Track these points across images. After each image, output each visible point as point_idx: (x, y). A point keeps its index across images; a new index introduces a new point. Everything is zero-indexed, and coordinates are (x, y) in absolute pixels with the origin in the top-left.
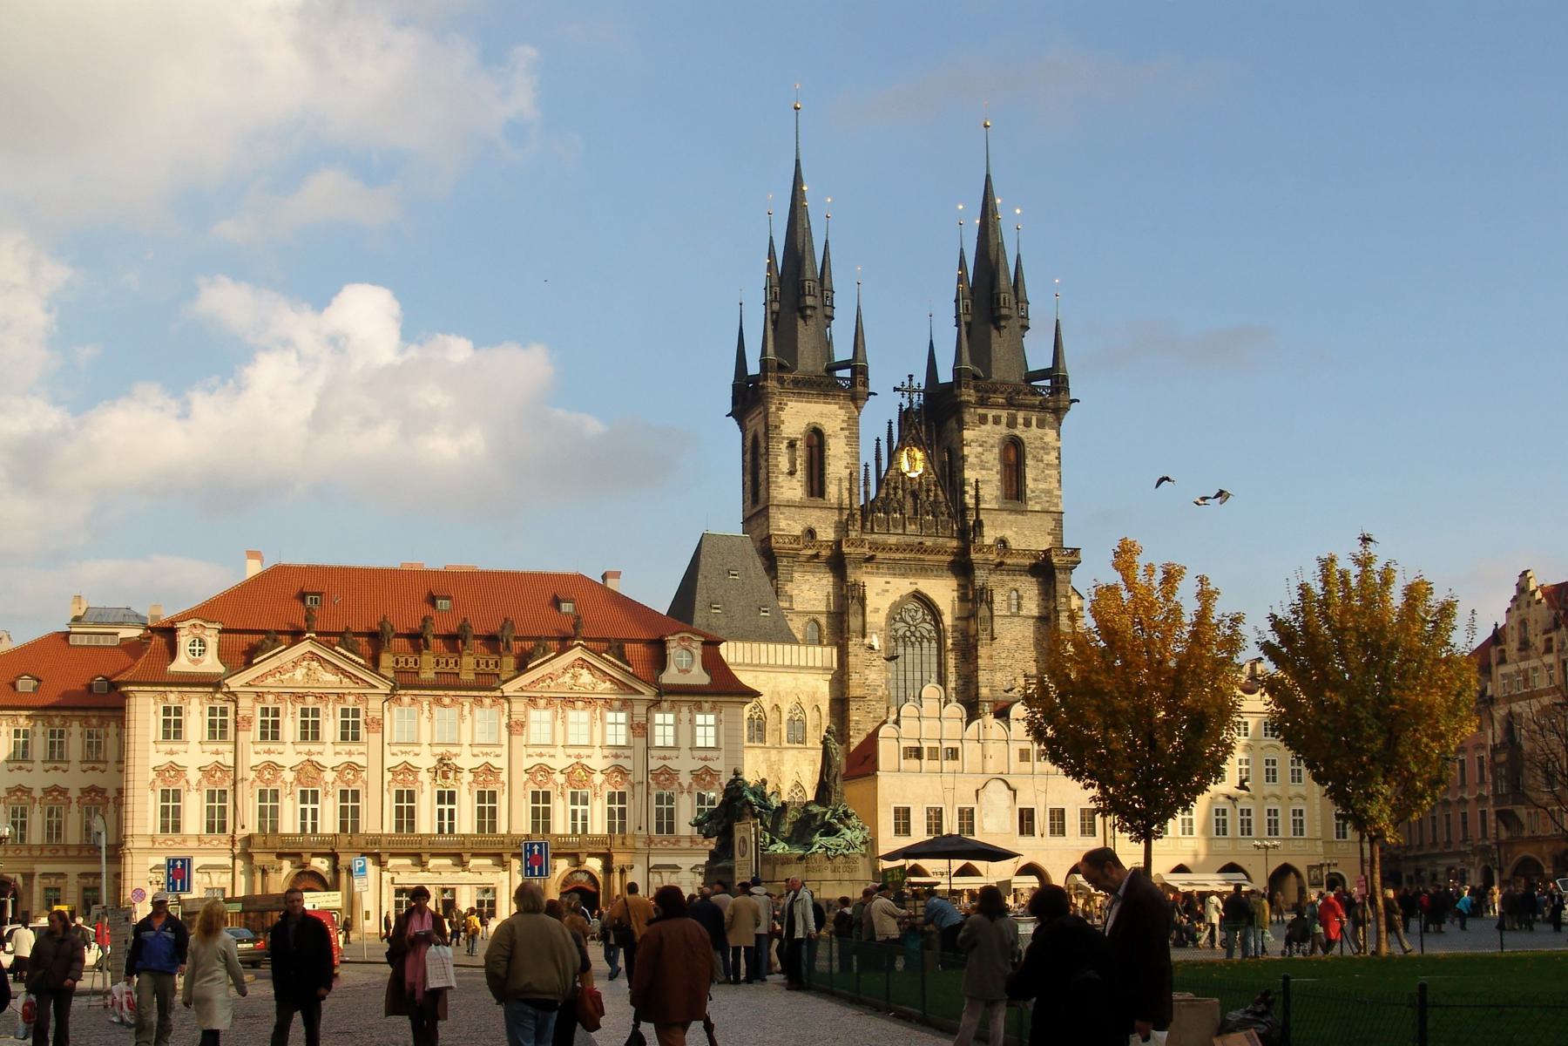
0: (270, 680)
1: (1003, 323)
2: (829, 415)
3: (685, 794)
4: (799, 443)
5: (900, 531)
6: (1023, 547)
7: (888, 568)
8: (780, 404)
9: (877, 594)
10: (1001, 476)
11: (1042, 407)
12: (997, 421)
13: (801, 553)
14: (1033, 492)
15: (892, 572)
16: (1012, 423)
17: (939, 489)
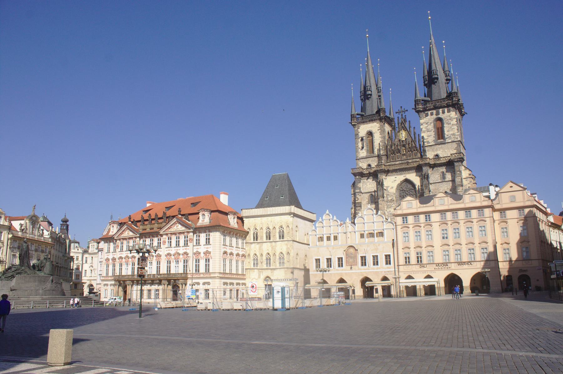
0: (122, 236)
1: (436, 80)
2: (374, 127)
3: (202, 259)
4: (364, 138)
5: (399, 159)
6: (446, 156)
7: (396, 173)
8: (358, 127)
9: (392, 182)
10: (435, 133)
11: (448, 106)
12: (432, 114)
13: (365, 173)
14: (447, 135)
15: (397, 173)
17: (413, 142)
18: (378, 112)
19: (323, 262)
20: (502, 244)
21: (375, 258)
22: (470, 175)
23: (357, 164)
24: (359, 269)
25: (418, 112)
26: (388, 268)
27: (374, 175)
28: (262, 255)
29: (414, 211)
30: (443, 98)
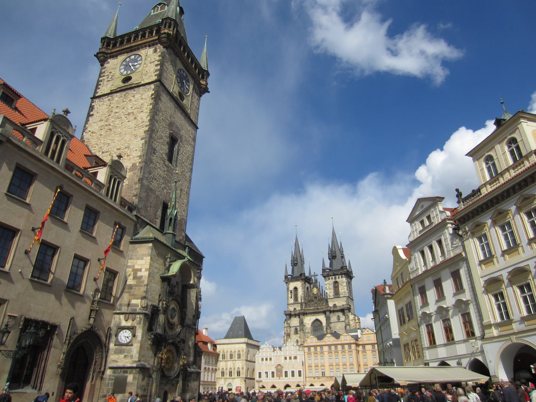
2: (298, 284)
11: (341, 274)
12: (332, 279)
16: (335, 278)
18: (301, 275)
19: (263, 375)
20: (364, 365)
21: (293, 372)
22: (354, 318)
23: (288, 308)
24: (284, 379)
25: (325, 277)
26: (300, 379)
27: (298, 315)
28: (227, 369)
29: (314, 344)
30: (339, 269)
